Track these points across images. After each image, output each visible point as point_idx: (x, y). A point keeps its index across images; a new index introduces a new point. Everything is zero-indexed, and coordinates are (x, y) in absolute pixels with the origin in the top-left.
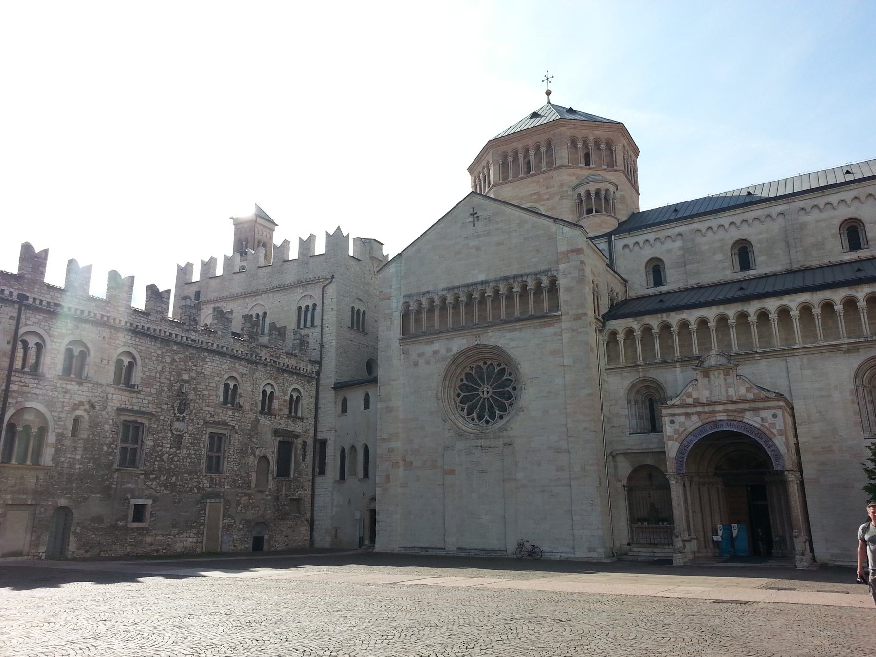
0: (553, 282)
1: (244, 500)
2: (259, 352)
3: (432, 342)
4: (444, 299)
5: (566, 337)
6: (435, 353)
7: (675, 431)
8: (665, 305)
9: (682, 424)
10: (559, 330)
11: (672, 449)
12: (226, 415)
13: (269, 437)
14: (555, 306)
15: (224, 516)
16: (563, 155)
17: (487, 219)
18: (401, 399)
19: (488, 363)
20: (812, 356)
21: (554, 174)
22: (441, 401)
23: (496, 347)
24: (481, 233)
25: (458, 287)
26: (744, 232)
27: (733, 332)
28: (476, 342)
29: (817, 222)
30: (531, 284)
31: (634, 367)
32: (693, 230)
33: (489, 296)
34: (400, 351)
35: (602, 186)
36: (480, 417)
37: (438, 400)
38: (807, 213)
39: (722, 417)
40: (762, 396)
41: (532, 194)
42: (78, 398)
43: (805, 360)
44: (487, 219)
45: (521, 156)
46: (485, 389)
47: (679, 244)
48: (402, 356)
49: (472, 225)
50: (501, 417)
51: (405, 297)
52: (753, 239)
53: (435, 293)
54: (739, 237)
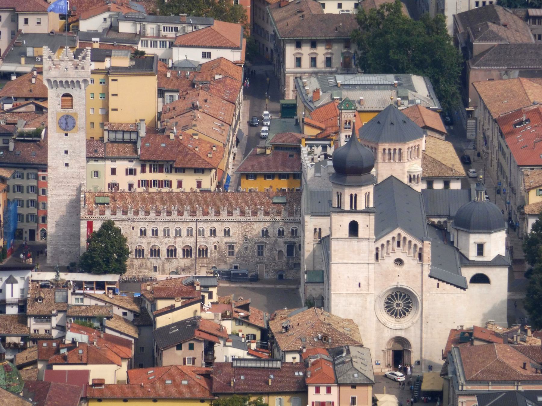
1: (273, 264)
2: (275, 217)
12: (264, 240)
13: (282, 244)
15: (265, 268)
42: (214, 241)
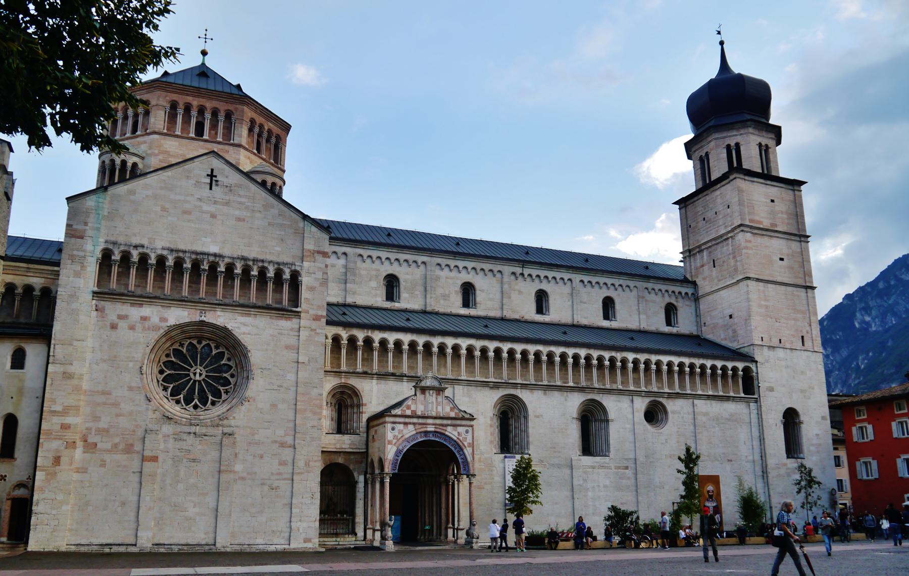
0: (295, 275)
3: (141, 305)
4: (161, 260)
5: (304, 334)
6: (144, 319)
7: (395, 436)
8: (409, 325)
9: (400, 431)
10: (297, 326)
11: (390, 453)
14: (295, 299)
16: (242, 134)
17: (228, 188)
18: (87, 365)
19: (204, 343)
20: (470, 387)
21: (231, 148)
22: (145, 376)
23: (225, 329)
24: (220, 200)
25: (184, 252)
26: (395, 269)
27: (420, 357)
28: (201, 319)
29: (447, 278)
30: (271, 274)
31: (338, 373)
32: (356, 253)
33: (223, 272)
34: (92, 305)
36: (188, 401)
37: (142, 374)
38: (442, 269)
39: (431, 428)
40: (461, 416)
43: (465, 389)
44: (228, 188)
45: (194, 113)
46: (198, 371)
47: (342, 261)
48: (94, 313)
49: (208, 187)
50: (213, 403)
51: (106, 242)
52: (402, 277)
53: (152, 249)
54: (390, 272)
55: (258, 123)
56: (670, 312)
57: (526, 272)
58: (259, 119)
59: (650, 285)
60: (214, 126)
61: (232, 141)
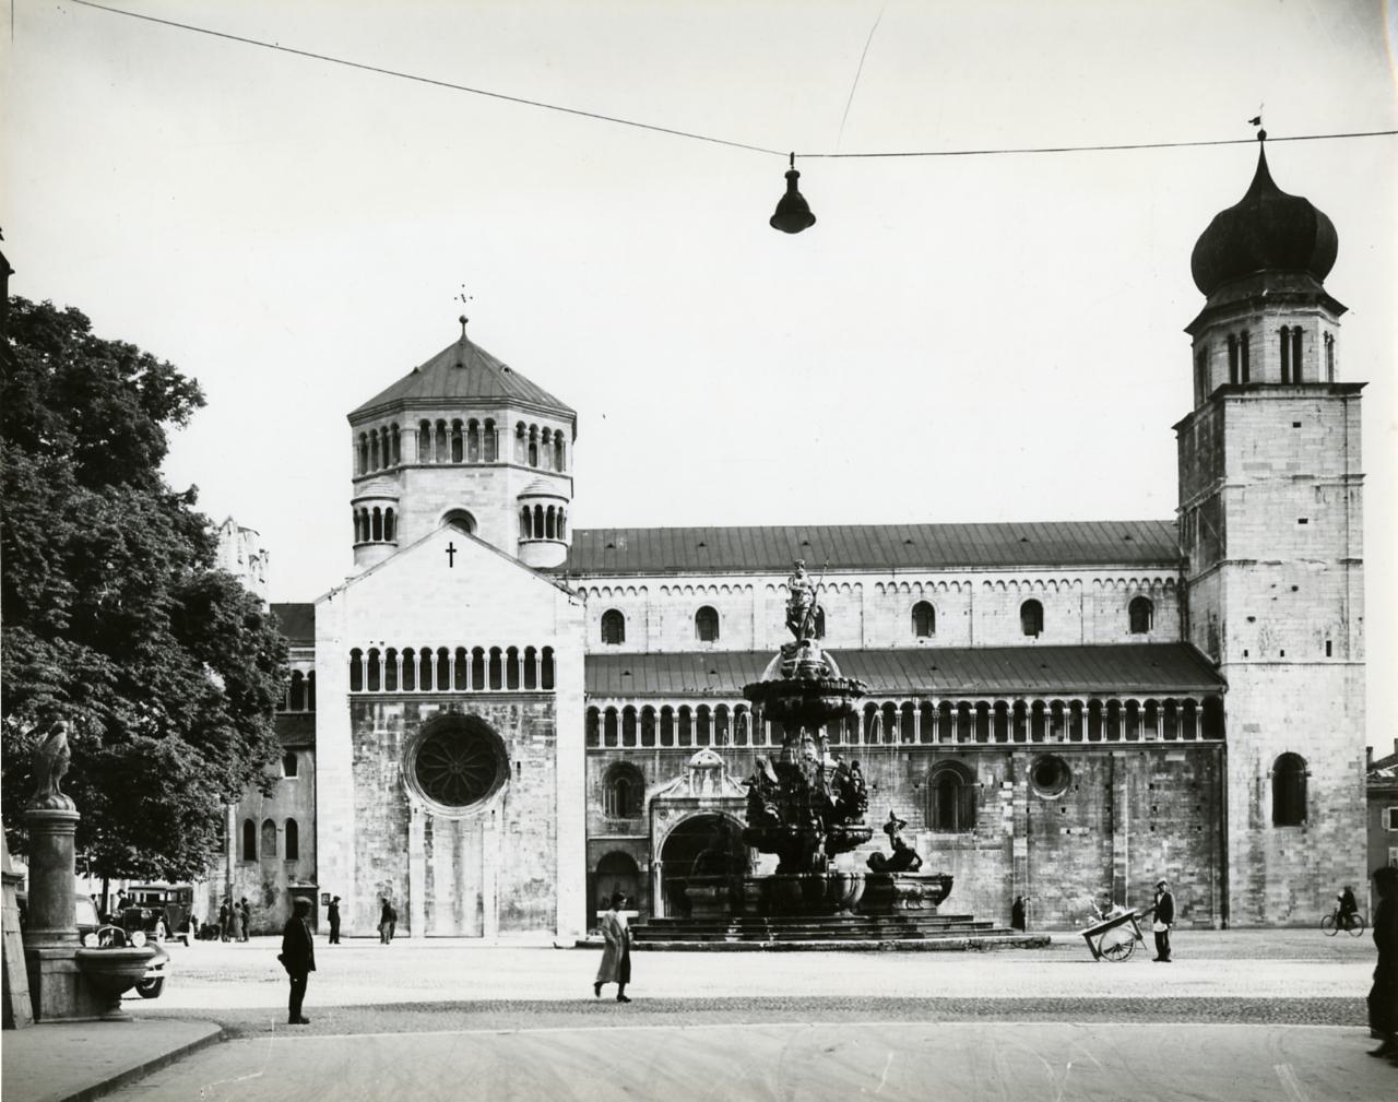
0: (548, 651)
11: (659, 840)
14: (549, 682)
16: (509, 448)
21: (496, 472)
35: (557, 503)
41: (464, 493)
52: (720, 610)
55: (528, 425)
56: (1140, 612)
57: (898, 579)
58: (529, 419)
59: (1103, 575)
60: (475, 442)
61: (496, 461)
